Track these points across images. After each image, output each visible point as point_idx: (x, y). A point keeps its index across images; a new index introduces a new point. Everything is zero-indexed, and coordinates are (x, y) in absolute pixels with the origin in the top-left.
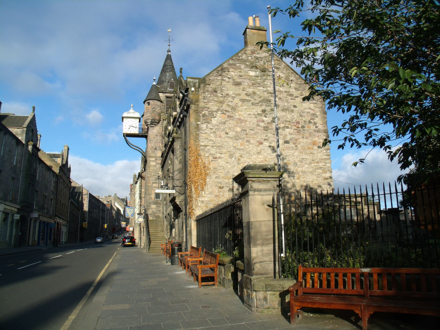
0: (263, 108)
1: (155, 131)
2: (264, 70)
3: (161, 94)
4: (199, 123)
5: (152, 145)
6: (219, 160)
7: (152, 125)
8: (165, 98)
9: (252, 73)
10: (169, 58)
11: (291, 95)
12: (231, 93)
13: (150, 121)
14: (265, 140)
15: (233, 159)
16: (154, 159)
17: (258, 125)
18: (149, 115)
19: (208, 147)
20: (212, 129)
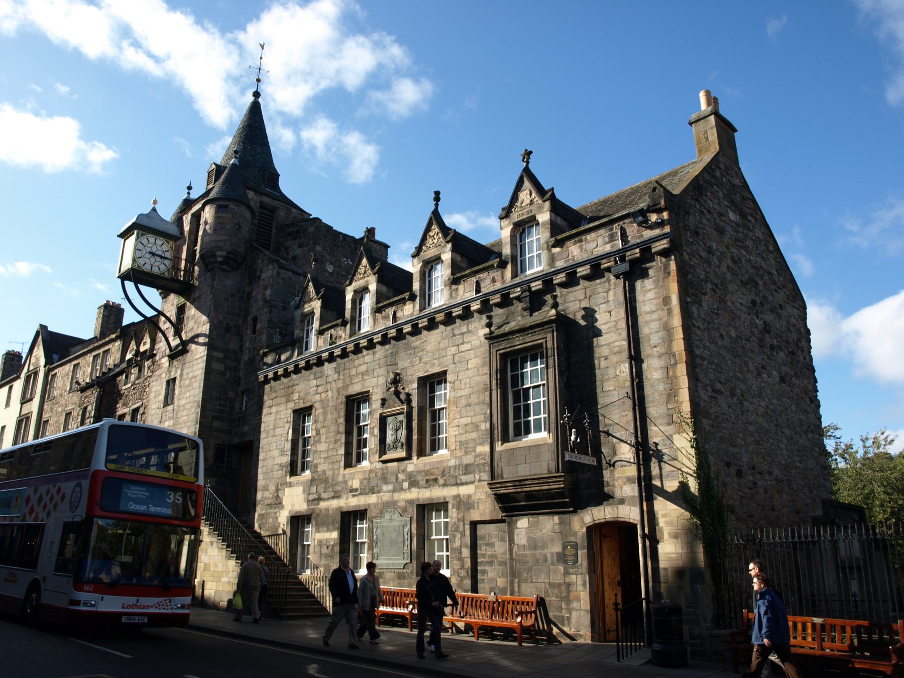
0: (753, 297)
1: (229, 282)
2: (743, 216)
3: (251, 194)
4: (689, 300)
5: (221, 318)
6: (719, 397)
7: (225, 267)
8: (258, 205)
9: (732, 216)
10: (255, 111)
11: (774, 283)
12: (714, 246)
13: (225, 253)
14: (763, 367)
15: (735, 398)
16: (221, 355)
17: (752, 333)
18: (224, 237)
19: (706, 363)
20: (704, 320)
